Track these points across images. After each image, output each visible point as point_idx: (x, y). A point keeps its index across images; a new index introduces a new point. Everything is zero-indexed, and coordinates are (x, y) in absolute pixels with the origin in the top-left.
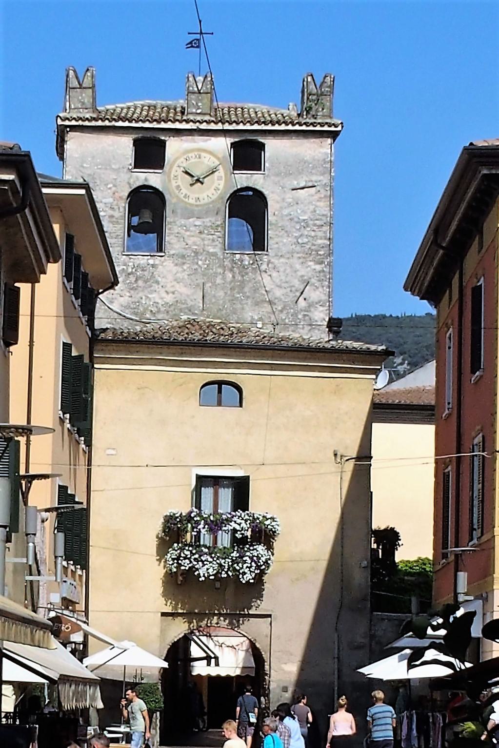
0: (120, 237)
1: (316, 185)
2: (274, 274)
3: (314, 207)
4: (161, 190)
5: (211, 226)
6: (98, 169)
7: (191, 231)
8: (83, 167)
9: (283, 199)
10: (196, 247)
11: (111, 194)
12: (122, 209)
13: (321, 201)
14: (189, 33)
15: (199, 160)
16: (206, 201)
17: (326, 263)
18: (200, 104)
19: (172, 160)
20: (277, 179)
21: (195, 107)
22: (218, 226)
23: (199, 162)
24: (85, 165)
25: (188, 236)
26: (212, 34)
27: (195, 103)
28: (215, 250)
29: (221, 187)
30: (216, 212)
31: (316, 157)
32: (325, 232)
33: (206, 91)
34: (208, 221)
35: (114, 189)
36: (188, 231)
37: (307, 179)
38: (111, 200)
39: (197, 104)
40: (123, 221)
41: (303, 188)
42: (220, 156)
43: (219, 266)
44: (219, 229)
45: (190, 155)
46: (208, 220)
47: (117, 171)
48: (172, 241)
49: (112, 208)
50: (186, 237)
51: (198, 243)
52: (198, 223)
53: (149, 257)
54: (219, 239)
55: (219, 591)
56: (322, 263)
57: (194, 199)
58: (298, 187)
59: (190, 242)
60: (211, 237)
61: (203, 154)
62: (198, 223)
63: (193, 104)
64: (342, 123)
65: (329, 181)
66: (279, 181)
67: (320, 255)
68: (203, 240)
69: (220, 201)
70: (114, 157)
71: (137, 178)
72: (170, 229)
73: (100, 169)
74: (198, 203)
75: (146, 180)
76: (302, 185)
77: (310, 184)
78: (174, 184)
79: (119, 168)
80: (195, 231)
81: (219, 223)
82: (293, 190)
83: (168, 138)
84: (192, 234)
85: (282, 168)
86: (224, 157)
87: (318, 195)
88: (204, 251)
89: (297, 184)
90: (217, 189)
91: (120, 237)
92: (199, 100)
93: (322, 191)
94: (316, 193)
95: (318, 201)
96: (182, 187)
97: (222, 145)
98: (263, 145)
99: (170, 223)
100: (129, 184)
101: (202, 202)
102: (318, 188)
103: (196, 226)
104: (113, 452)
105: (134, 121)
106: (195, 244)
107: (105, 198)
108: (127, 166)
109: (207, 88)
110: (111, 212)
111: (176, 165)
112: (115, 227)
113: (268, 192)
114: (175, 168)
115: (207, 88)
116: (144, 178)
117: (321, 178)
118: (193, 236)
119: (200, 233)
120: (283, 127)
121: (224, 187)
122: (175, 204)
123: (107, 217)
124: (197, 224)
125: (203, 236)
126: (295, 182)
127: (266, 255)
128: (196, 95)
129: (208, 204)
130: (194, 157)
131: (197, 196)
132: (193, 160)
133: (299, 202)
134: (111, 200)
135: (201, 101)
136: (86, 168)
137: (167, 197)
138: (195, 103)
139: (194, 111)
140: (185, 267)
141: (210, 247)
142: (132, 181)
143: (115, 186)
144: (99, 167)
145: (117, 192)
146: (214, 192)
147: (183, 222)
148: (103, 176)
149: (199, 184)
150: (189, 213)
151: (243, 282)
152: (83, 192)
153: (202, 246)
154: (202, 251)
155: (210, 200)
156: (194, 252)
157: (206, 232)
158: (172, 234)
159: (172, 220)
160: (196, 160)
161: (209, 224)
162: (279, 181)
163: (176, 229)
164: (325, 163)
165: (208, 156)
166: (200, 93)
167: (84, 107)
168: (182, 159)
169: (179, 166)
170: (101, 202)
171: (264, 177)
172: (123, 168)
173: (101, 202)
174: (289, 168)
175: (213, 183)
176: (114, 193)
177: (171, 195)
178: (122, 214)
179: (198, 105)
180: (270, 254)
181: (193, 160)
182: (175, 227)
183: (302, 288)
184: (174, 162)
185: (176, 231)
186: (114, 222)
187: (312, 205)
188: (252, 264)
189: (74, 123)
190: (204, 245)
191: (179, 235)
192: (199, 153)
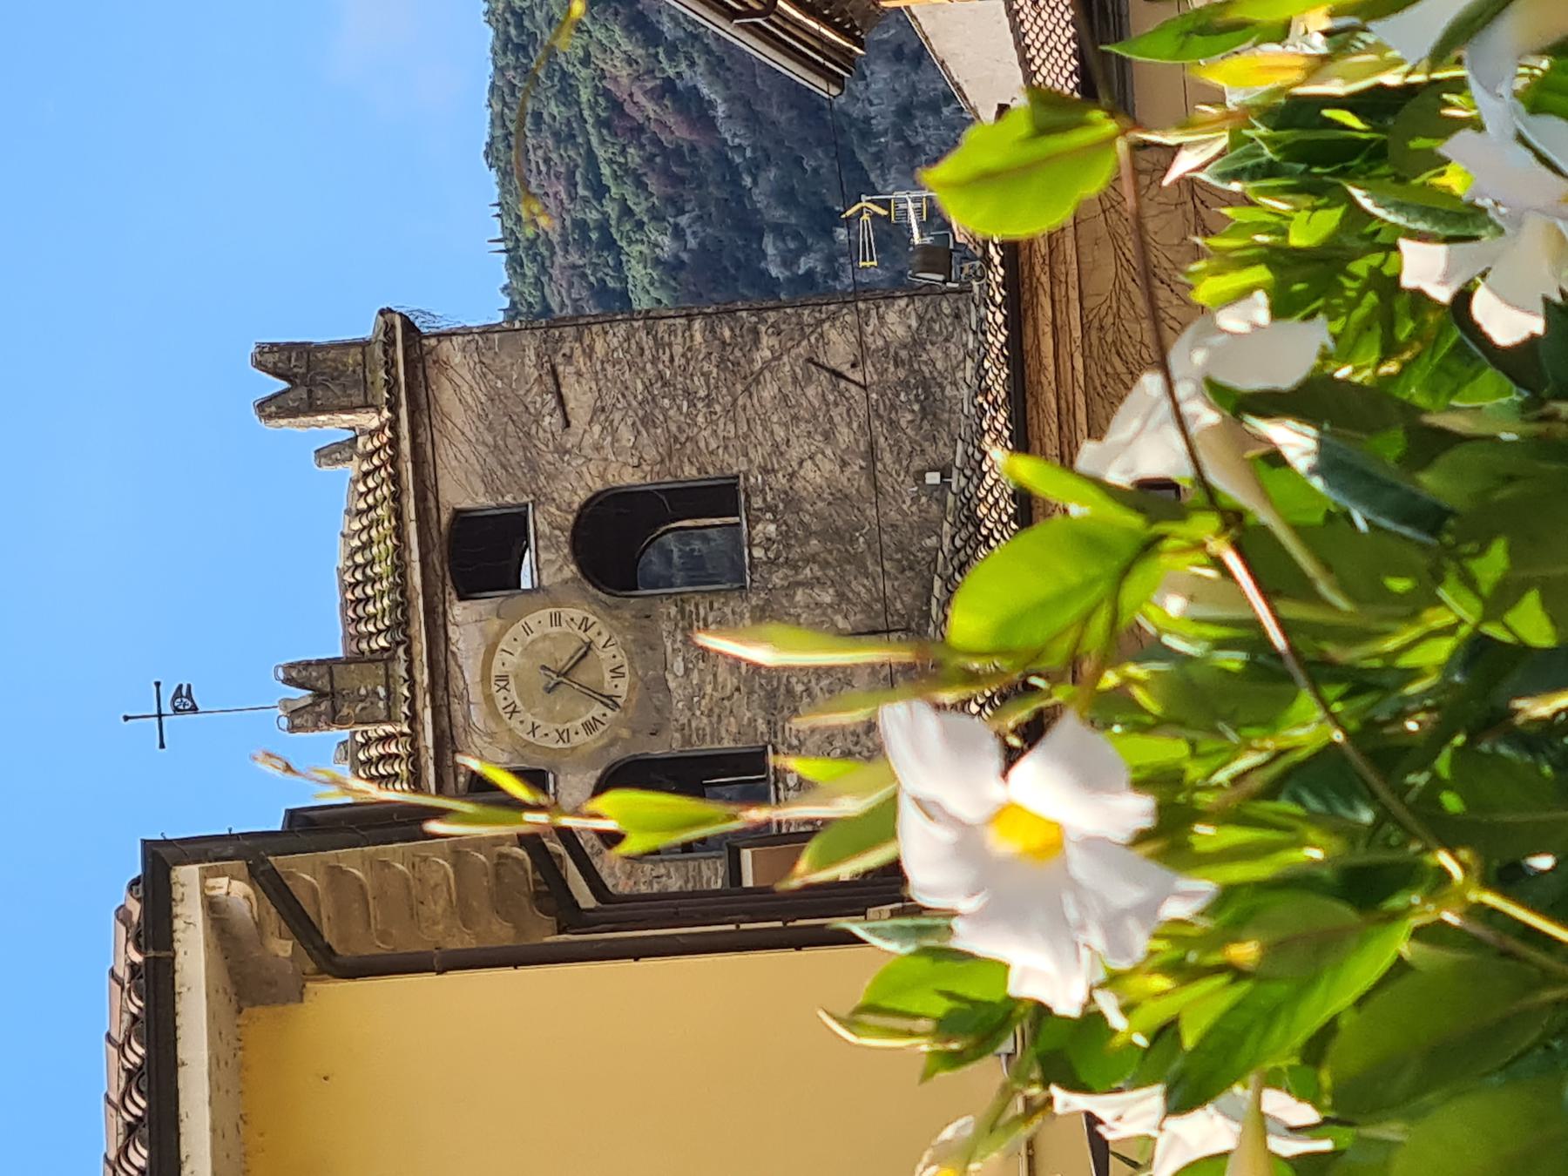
2: (794, 453)
4: (599, 772)
5: (683, 629)
7: (704, 682)
15: (512, 680)
17: (754, 319)
22: (682, 611)
23: (516, 676)
25: (715, 689)
27: (360, 706)
29: (578, 614)
30: (646, 622)
32: (672, 331)
33: (327, 677)
43: (791, 597)
44: (690, 607)
45: (501, 704)
48: (734, 729)
52: (679, 666)
53: (781, 785)
54: (716, 605)
56: (755, 332)
57: (616, 681)
61: (497, 669)
62: (679, 666)
63: (363, 709)
67: (734, 336)
74: (626, 670)
77: (549, 380)
78: (581, 738)
81: (673, 610)
84: (709, 678)
96: (588, 717)
98: (459, 515)
99: (687, 741)
103: (686, 669)
118: (715, 675)
121: (573, 606)
127: (747, 479)
130: (503, 693)
131: (608, 676)
138: (360, 706)
139: (381, 704)
140: (799, 688)
147: (680, 705)
151: (821, 535)
152: (746, 855)
160: (512, 686)
161: (679, 637)
165: (499, 657)
168: (514, 723)
179: (367, 696)
180: (744, 468)
181: (514, 695)
183: (824, 377)
185: (705, 720)
188: (774, 513)
191: (717, 710)
192: (493, 679)
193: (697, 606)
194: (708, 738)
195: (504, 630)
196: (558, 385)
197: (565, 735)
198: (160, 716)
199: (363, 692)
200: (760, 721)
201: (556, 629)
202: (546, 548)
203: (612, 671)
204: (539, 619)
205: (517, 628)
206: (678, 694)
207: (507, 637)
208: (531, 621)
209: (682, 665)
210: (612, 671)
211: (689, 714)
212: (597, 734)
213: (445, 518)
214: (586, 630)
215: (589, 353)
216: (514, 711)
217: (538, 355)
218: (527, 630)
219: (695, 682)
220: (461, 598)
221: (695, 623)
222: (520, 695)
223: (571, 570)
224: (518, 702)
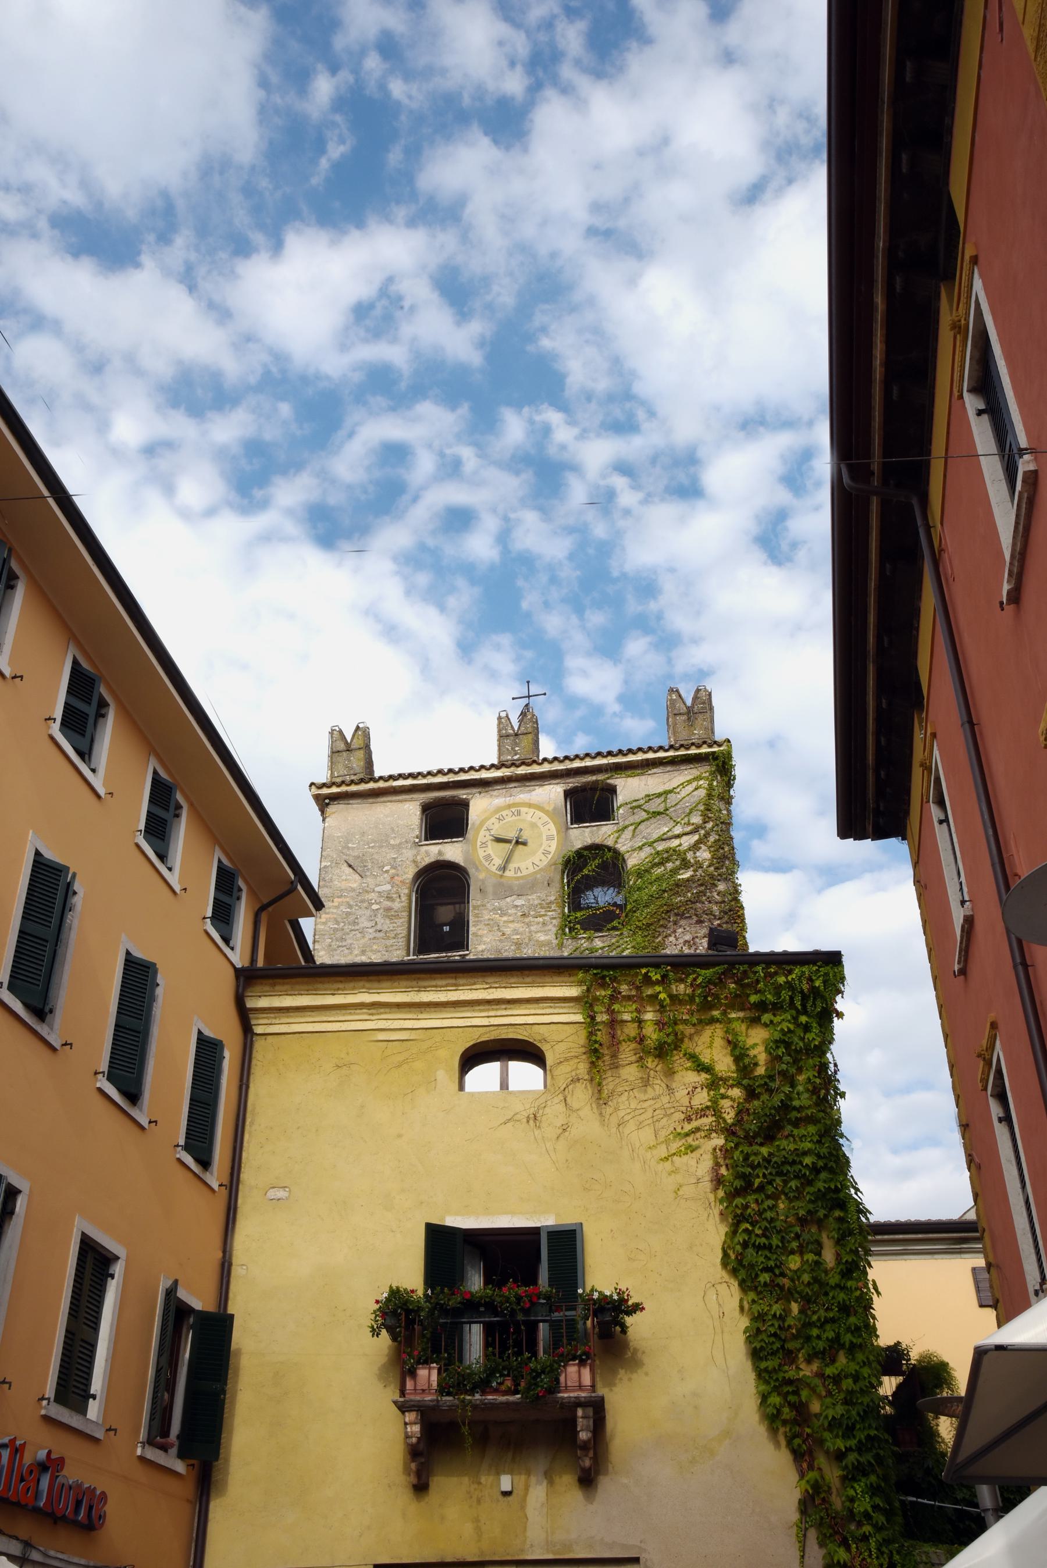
0: (400, 936)
4: (462, 864)
5: (540, 904)
6: (369, 847)
7: (510, 916)
8: (348, 848)
10: (518, 937)
11: (388, 879)
12: (404, 898)
14: (513, 699)
16: (531, 870)
19: (478, 822)
24: (350, 845)
25: (505, 922)
26: (545, 694)
27: (510, 748)
28: (547, 938)
30: (546, 883)
33: (525, 731)
34: (534, 898)
35: (393, 871)
36: (505, 915)
38: (388, 887)
39: (512, 749)
40: (405, 914)
42: (551, 809)
44: (553, 907)
45: (504, 813)
46: (534, 896)
47: (398, 847)
48: (480, 933)
49: (389, 898)
50: (501, 924)
51: (521, 929)
52: (520, 902)
54: (554, 921)
55: (510, 1498)
59: (508, 931)
60: (541, 919)
61: (524, 810)
63: (508, 749)
68: (528, 925)
69: (553, 867)
70: (393, 830)
71: (427, 852)
72: (476, 916)
73: (372, 847)
74: (519, 874)
75: (440, 853)
79: (400, 844)
80: (516, 914)
83: (471, 796)
84: (511, 918)
86: (555, 809)
88: (530, 940)
90: (546, 853)
91: (400, 936)
97: (553, 793)
98: (612, 790)
100: (414, 861)
101: (525, 873)
103: (517, 906)
104: (281, 1194)
106: (516, 932)
107: (377, 885)
108: (412, 840)
109: (526, 728)
110: (389, 904)
111: (484, 828)
112: (393, 923)
114: (482, 833)
115: (526, 728)
116: (437, 852)
118: (513, 921)
119: (524, 915)
120: (640, 756)
122: (483, 881)
123: (382, 910)
124: (517, 904)
125: (527, 920)
128: (512, 738)
129: (535, 873)
132: (508, 819)
134: (388, 887)
135: (517, 745)
136: (353, 849)
137: (472, 871)
138: (510, 748)
139: (509, 757)
141: (539, 934)
143: (393, 867)
144: (371, 845)
145: (398, 875)
146: (543, 858)
148: (376, 856)
149: (520, 847)
150: (505, 890)
153: (527, 934)
154: (527, 940)
155: (537, 868)
156: (516, 944)
157: (532, 913)
158: (481, 921)
159: (479, 903)
161: (536, 902)
163: (486, 916)
167: (352, 772)
168: (493, 820)
169: (488, 830)
170: (374, 891)
172: (406, 842)
173: (374, 891)
175: (541, 845)
176: (392, 878)
177: (477, 869)
178: (405, 904)
181: (508, 819)
182: (485, 912)
185: (486, 917)
186: (392, 916)
189: (335, 790)
190: (530, 932)
193: (554, 910)
194: (476, 919)
195: (546, 812)
197: (484, 845)
198: (529, 697)
199: (517, 749)
200: (484, 947)
201: (544, 837)
202: (592, 832)
203: (519, 868)
204: (552, 829)
205: (546, 818)
206: (503, 903)
207: (541, 814)
208: (552, 826)
209: (519, 904)
210: (519, 868)
211: (491, 908)
212: (483, 861)
216: (499, 819)
218: (545, 824)
219: (509, 911)
220: (565, 791)
221: (543, 910)
222: (509, 822)
223: (578, 845)
224: (504, 822)
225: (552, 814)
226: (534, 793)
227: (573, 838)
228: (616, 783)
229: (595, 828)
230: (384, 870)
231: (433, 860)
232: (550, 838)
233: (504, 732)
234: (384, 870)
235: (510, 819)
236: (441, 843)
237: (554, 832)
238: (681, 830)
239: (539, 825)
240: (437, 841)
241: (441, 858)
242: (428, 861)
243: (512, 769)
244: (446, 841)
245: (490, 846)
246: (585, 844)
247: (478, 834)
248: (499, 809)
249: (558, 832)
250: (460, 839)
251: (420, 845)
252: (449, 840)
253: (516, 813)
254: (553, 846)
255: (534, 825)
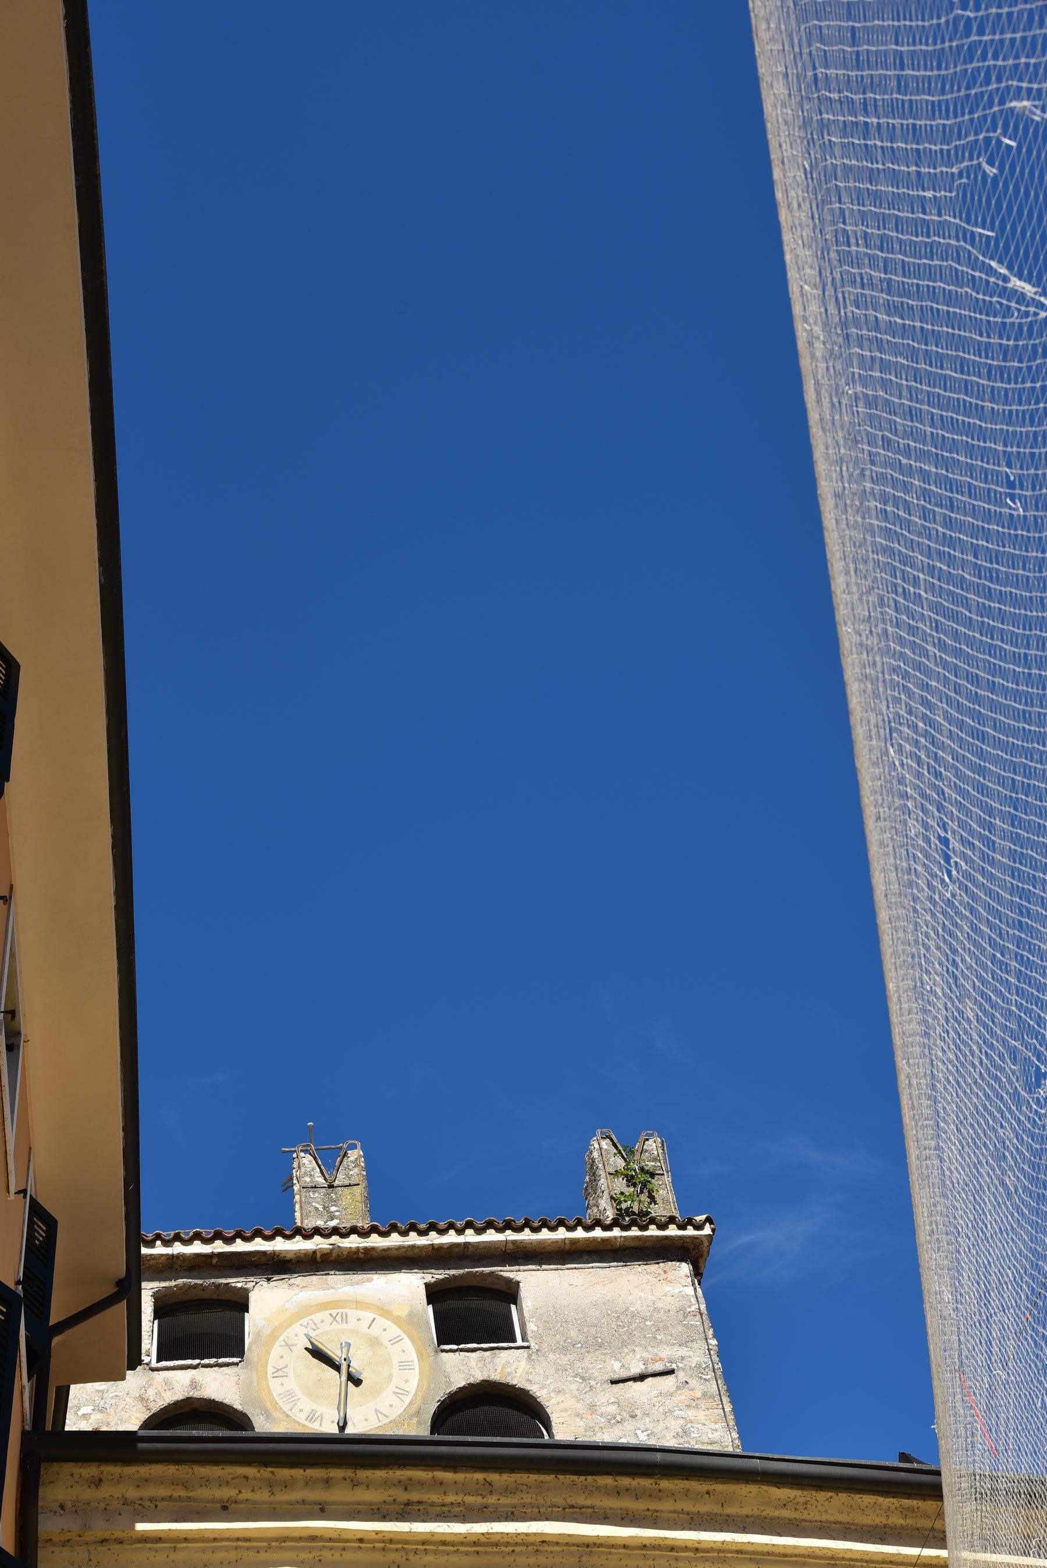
1: (674, 1366)
3: (681, 1422)
4: (238, 1406)
9: (592, 1408)
13: (697, 1407)
18: (333, 1209)
19: (267, 1331)
20: (564, 1360)
21: (321, 1216)
27: (320, 1208)
29: (413, 1385)
31: (659, 1305)
33: (347, 1182)
37: (646, 1355)
39: (324, 1208)
41: (641, 1378)
42: (403, 1313)
58: (625, 1374)
61: (352, 1313)
63: (317, 1209)
64: (709, 1220)
65: (707, 1359)
66: (571, 1364)
69: (415, 1420)
71: (167, 1382)
75: (194, 1385)
76: (637, 1369)
77: (659, 1367)
82: (614, 1382)
85: (573, 1333)
86: (411, 1315)
87: (683, 1396)
89: (623, 1366)
90: (400, 1392)
92: (332, 1200)
93: (694, 1383)
94: (678, 1388)
95: (688, 1406)
96: (299, 1393)
100: (141, 1399)
102: (681, 1375)
105: (158, 1243)
111: (280, 1341)
113: (545, 1391)
114: (276, 1350)
116: (187, 1382)
117: (684, 1351)
126: (617, 1365)
128: (323, 1190)
133: (638, 1412)
135: (335, 1202)
138: (320, 1208)
142: (151, 1393)
146: (396, 1402)
162: (571, 1364)
164: (685, 1317)
166: (331, 1186)
171: (529, 1357)
174: (593, 1331)
179: (329, 1212)
184: (273, 1337)
187: (677, 1418)
195: (397, 1321)
196: (654, 1375)
199: (333, 1209)
205: (395, 1331)
207: (387, 1323)
208: (407, 1343)
213: (511, 1275)
214: (395, 1393)
215: (693, 1404)
217: (683, 1358)
223: (459, 1381)
225: (408, 1324)
226: (368, 1285)
227: (448, 1368)
228: (518, 1279)
229: (488, 1353)
230: (80, 1413)
231: (179, 1396)
232: (404, 1366)
233: (308, 1179)
234: (80, 1413)
235: (328, 1328)
236: (195, 1367)
237: (413, 1355)
238: (643, 1367)
239: (385, 1342)
240: (189, 1362)
241: (196, 1394)
242: (169, 1398)
243: (335, 1239)
244: (206, 1361)
245: (292, 1375)
246: (472, 1380)
247: (268, 1353)
248: (305, 1311)
249: (420, 1356)
250: (236, 1360)
251: (153, 1370)
252: (212, 1361)
253: (339, 1318)
254: (412, 1381)
255: (374, 1343)
